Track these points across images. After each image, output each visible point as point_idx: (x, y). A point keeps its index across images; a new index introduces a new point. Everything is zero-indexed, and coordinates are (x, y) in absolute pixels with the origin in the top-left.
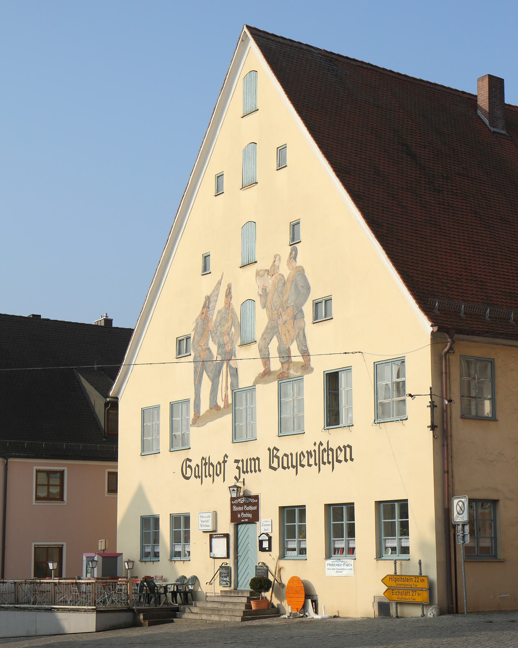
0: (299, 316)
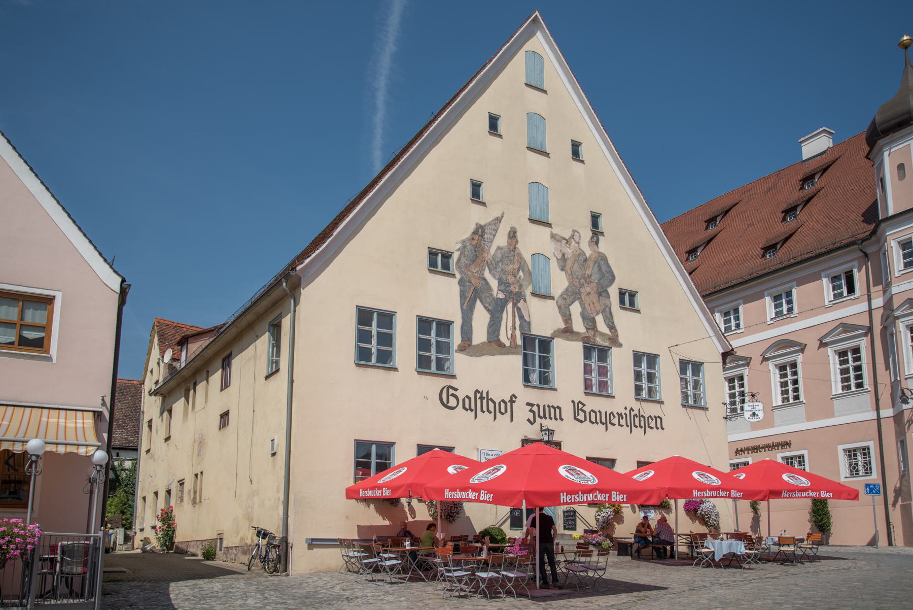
0: (604, 294)
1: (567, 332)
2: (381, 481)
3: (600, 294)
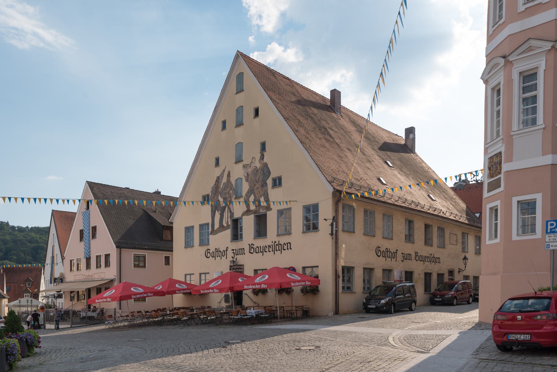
1: (248, 212)
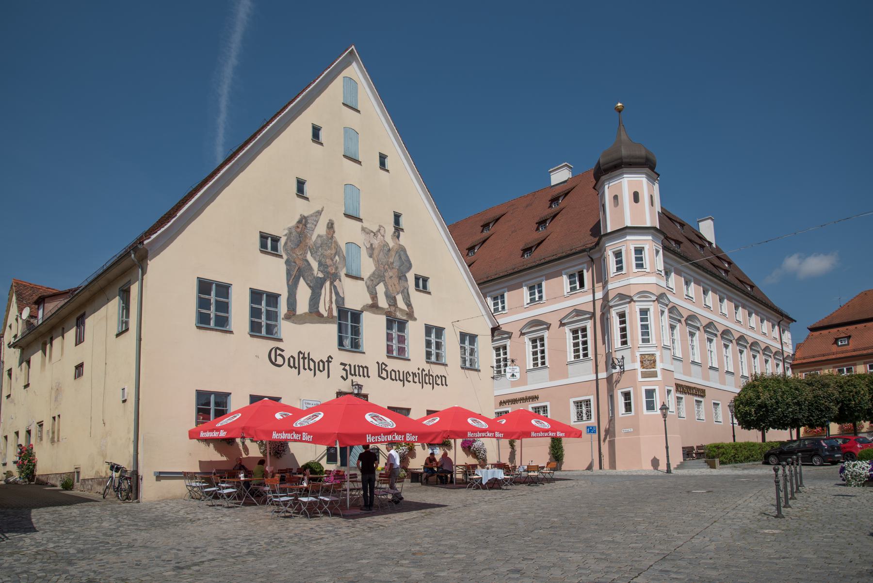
1: (374, 307)
2: (219, 425)
3: (400, 278)
